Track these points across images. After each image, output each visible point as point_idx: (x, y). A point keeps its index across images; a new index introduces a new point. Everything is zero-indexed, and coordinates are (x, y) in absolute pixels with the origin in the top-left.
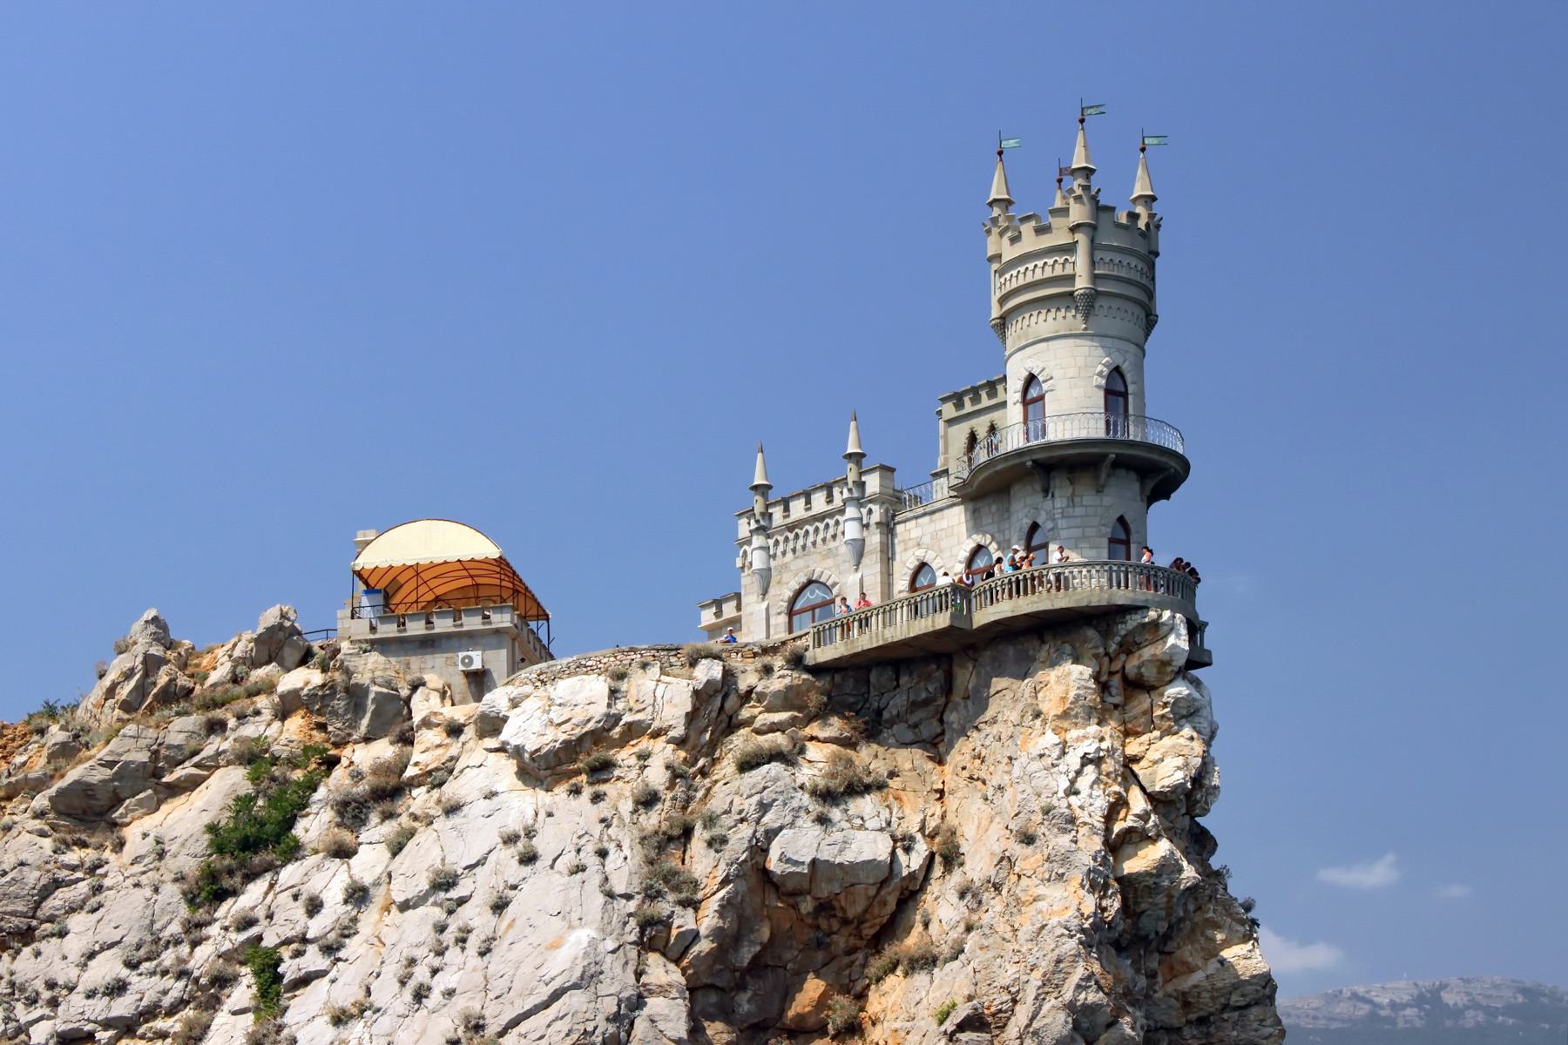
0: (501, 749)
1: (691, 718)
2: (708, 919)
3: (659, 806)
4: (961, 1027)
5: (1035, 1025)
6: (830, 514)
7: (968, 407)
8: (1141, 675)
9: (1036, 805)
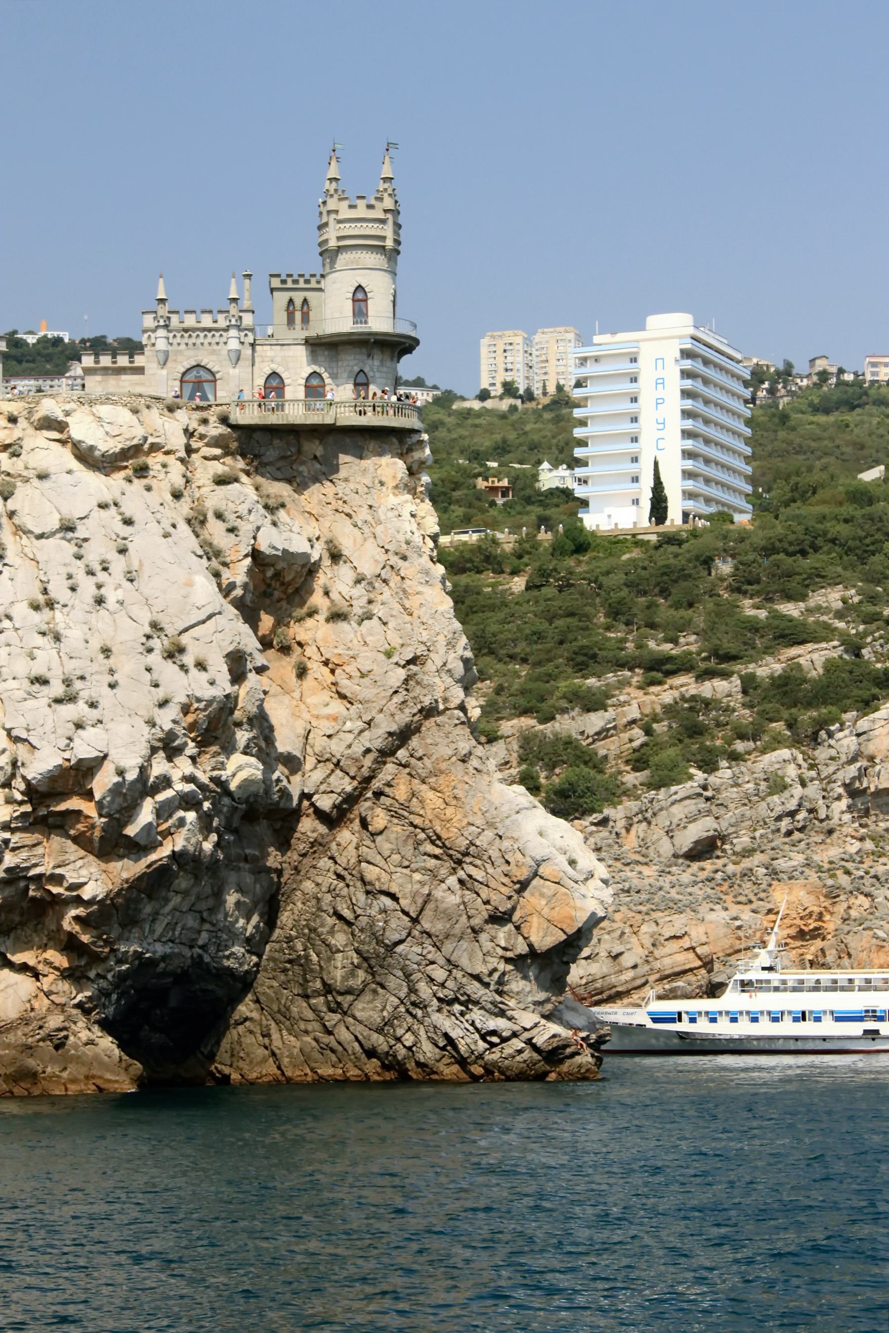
3: (183, 500)
6: (217, 330)
7: (290, 285)
9: (401, 538)
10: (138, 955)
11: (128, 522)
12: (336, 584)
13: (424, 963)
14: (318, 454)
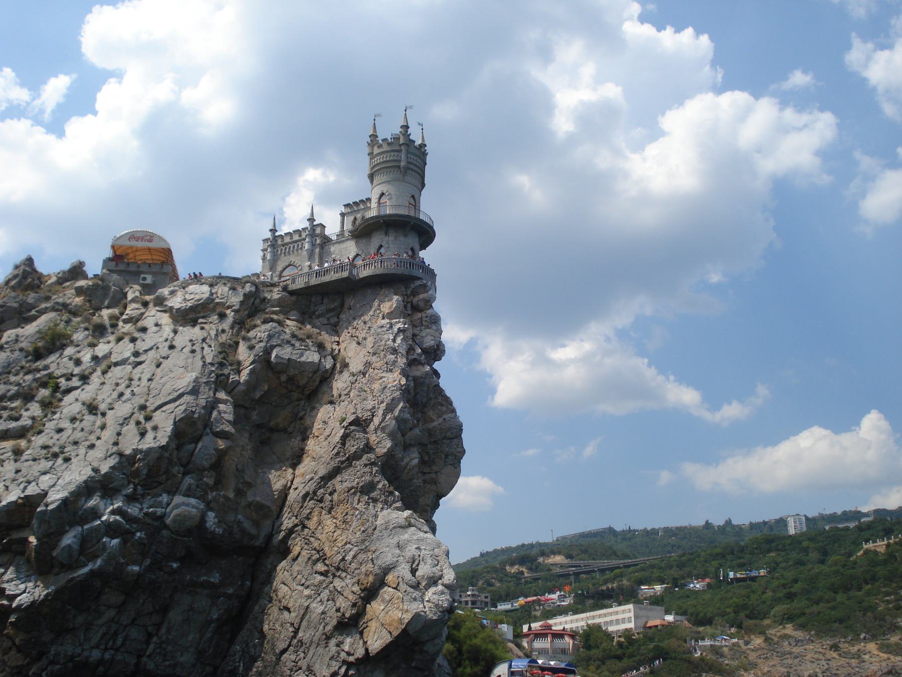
1: (242, 303)
2: (244, 376)
4: (351, 424)
5: (383, 424)
6: (300, 241)
10: (71, 658)
12: (339, 384)
13: (295, 669)
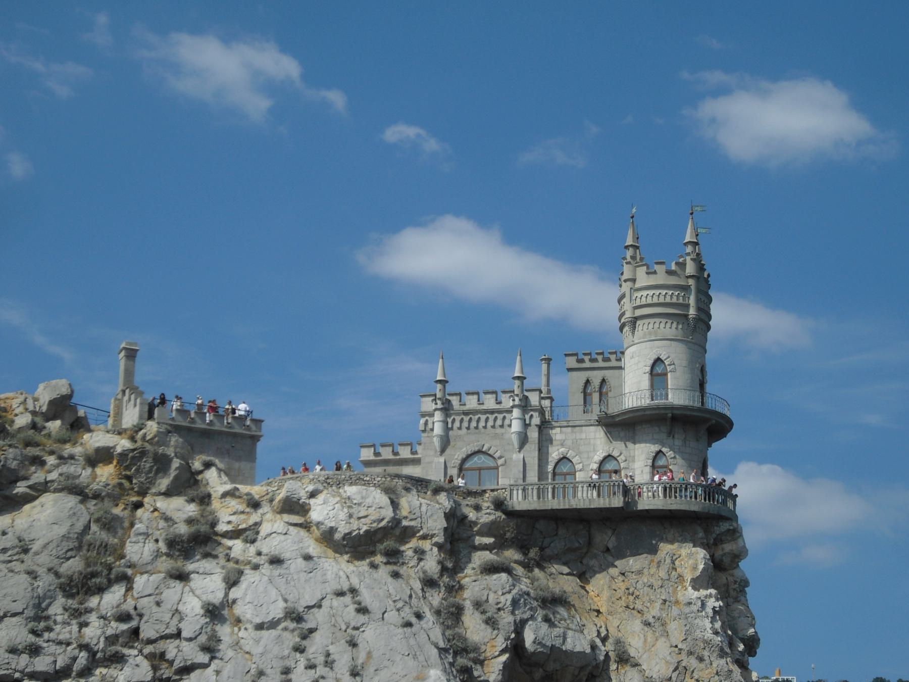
0: (306, 526)
6: (500, 412)
7: (587, 364)
8: (722, 560)
11: (362, 610)
14: (610, 546)
